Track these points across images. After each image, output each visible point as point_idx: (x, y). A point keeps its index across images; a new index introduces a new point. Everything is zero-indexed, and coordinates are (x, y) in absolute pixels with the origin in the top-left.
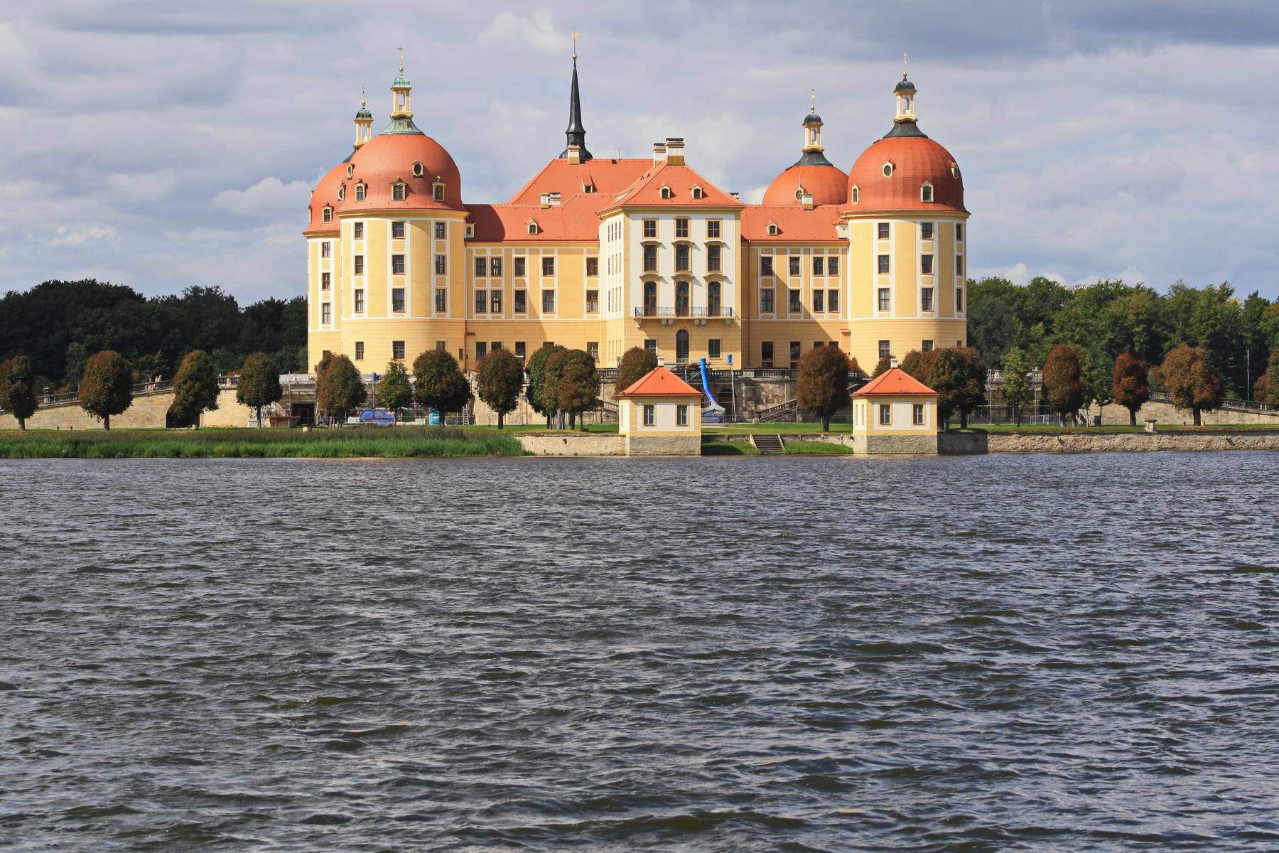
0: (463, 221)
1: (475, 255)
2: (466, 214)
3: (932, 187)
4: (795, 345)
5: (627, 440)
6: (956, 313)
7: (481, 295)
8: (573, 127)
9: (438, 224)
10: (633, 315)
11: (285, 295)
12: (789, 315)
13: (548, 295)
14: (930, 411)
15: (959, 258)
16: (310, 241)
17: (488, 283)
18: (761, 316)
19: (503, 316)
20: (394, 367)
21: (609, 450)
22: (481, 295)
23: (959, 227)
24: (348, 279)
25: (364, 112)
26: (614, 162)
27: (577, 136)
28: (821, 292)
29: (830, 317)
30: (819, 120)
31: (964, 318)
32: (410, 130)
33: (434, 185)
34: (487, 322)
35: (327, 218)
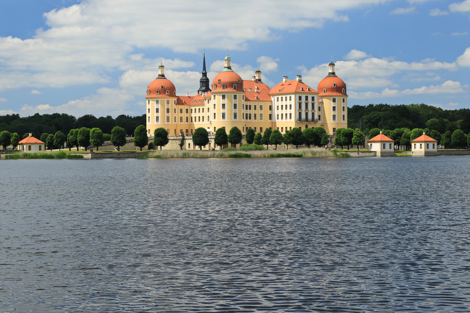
9: (234, 95)
11: (133, 114)
13: (261, 115)
17: (248, 112)
19: (251, 120)
21: (372, 155)
22: (247, 114)
25: (162, 65)
30: (260, 72)
32: (231, 71)
33: (234, 85)
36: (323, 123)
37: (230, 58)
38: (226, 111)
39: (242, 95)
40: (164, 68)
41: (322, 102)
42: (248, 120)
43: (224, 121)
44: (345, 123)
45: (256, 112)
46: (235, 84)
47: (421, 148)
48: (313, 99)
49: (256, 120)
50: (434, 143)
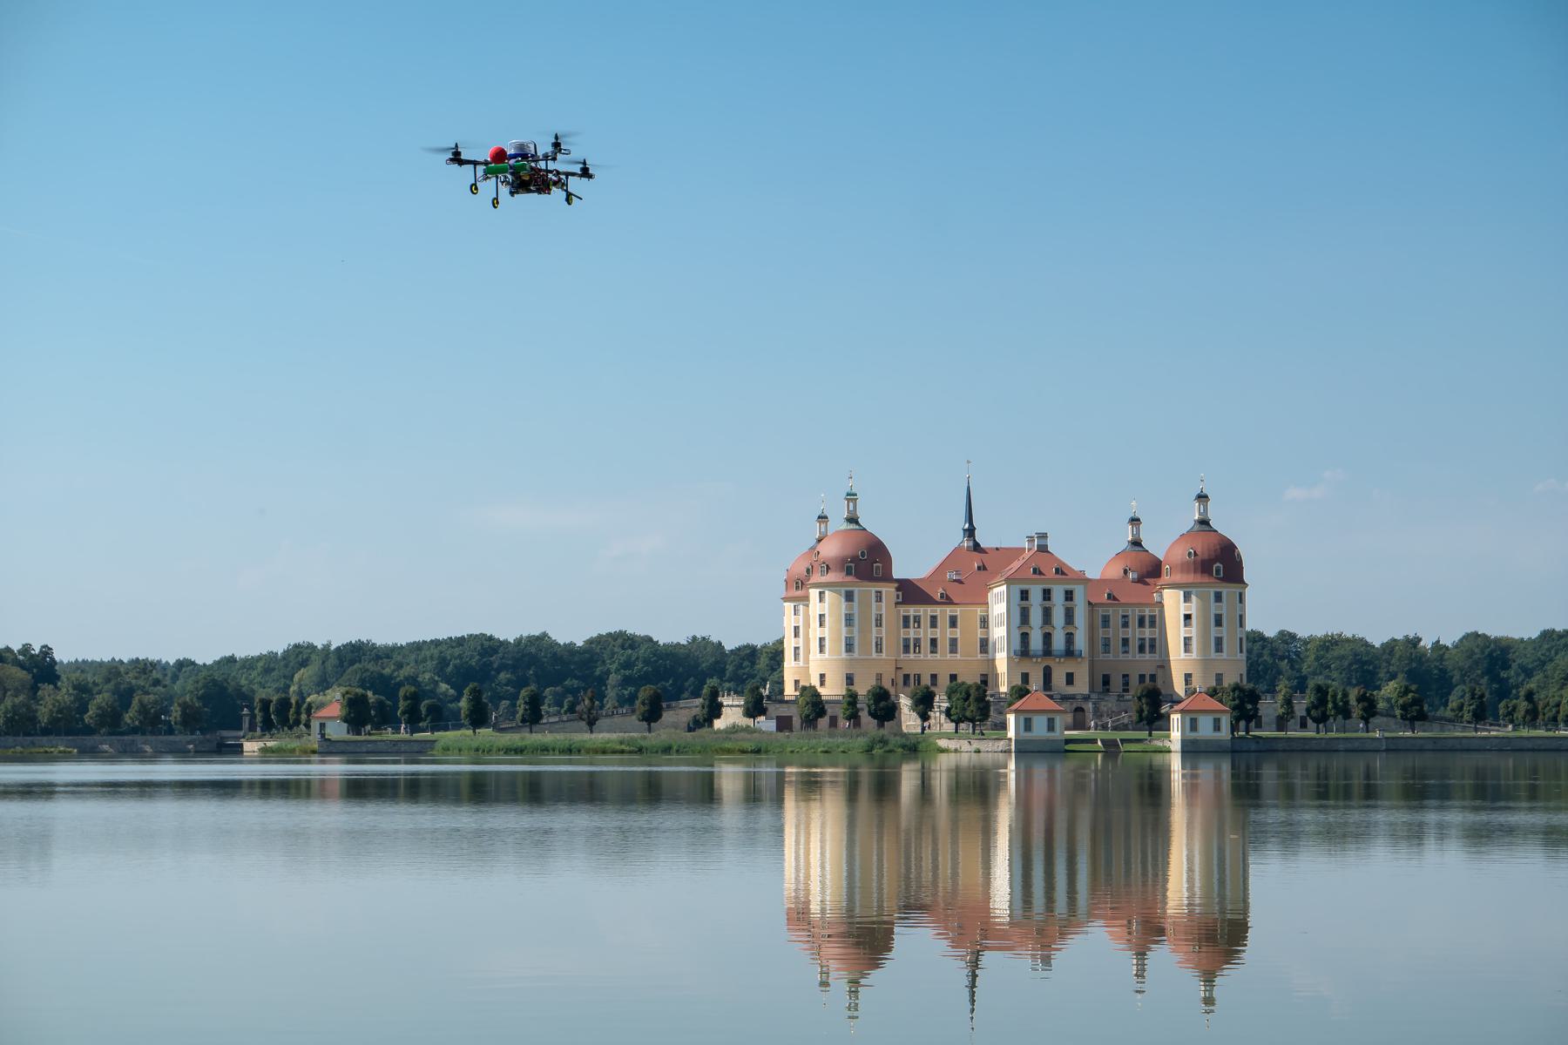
0: (894, 590)
1: (902, 613)
2: (896, 585)
3: (1221, 566)
4: (1125, 676)
5: (1013, 743)
6: (1239, 654)
7: (906, 641)
8: (967, 526)
9: (877, 592)
10: (1012, 654)
12: (1121, 655)
13: (954, 642)
14: (1225, 721)
15: (1241, 616)
16: (786, 604)
17: (912, 633)
18: (1102, 657)
20: (848, 690)
22: (906, 641)
23: (1241, 594)
24: (816, 631)
26: (997, 549)
27: (970, 532)
28: (1144, 639)
29: (1151, 657)
31: (1245, 658)
32: (857, 527)
34: (911, 660)
35: (797, 588)
36: (1163, 660)
37: (856, 495)
38: (826, 632)
39: (873, 590)
40: (827, 522)
41: (1161, 604)
42: (912, 656)
43: (821, 660)
44: (1238, 660)
45: (938, 633)
46: (851, 562)
47: (1217, 728)
48: (1069, 595)
49: (938, 656)
50: (1217, 716)
